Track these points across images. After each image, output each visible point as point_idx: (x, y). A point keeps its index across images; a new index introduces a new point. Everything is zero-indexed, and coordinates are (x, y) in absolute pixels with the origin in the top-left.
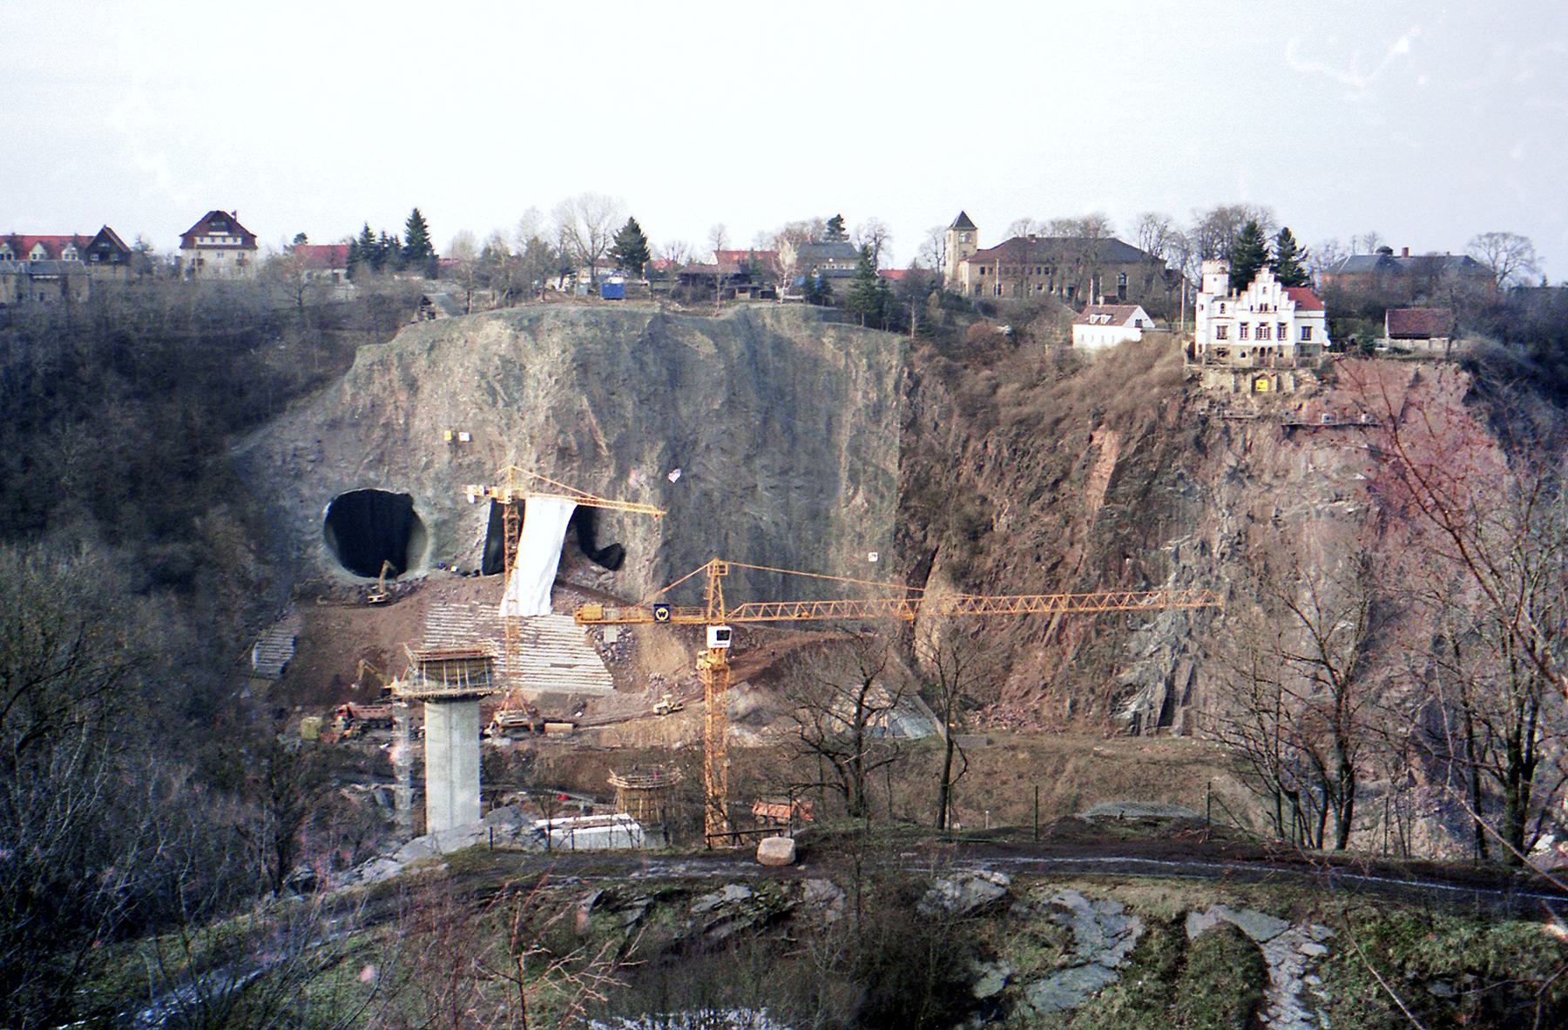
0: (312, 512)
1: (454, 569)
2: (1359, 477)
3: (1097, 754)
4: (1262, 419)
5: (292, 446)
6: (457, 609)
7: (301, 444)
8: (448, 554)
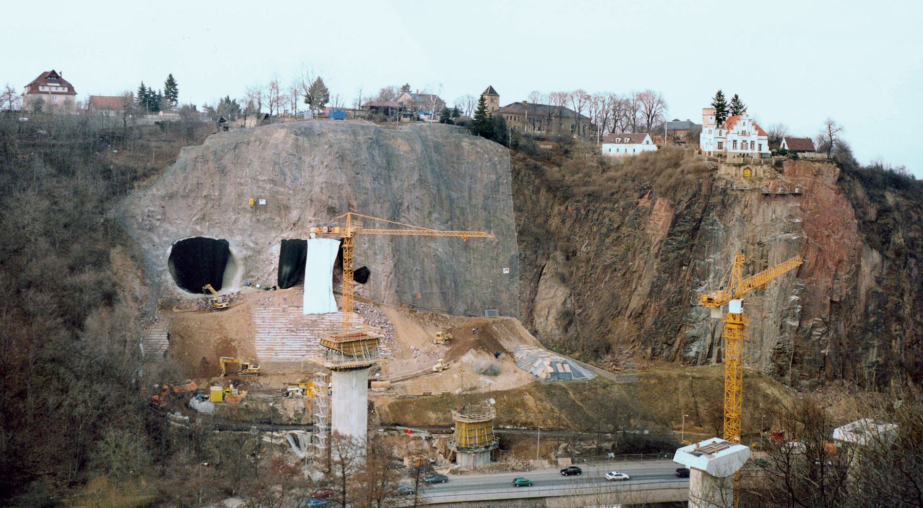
0: (161, 252)
1: (258, 286)
2: (797, 221)
3: (693, 378)
4: (753, 190)
5: (146, 210)
6: (274, 311)
7: (152, 209)
8: (252, 277)
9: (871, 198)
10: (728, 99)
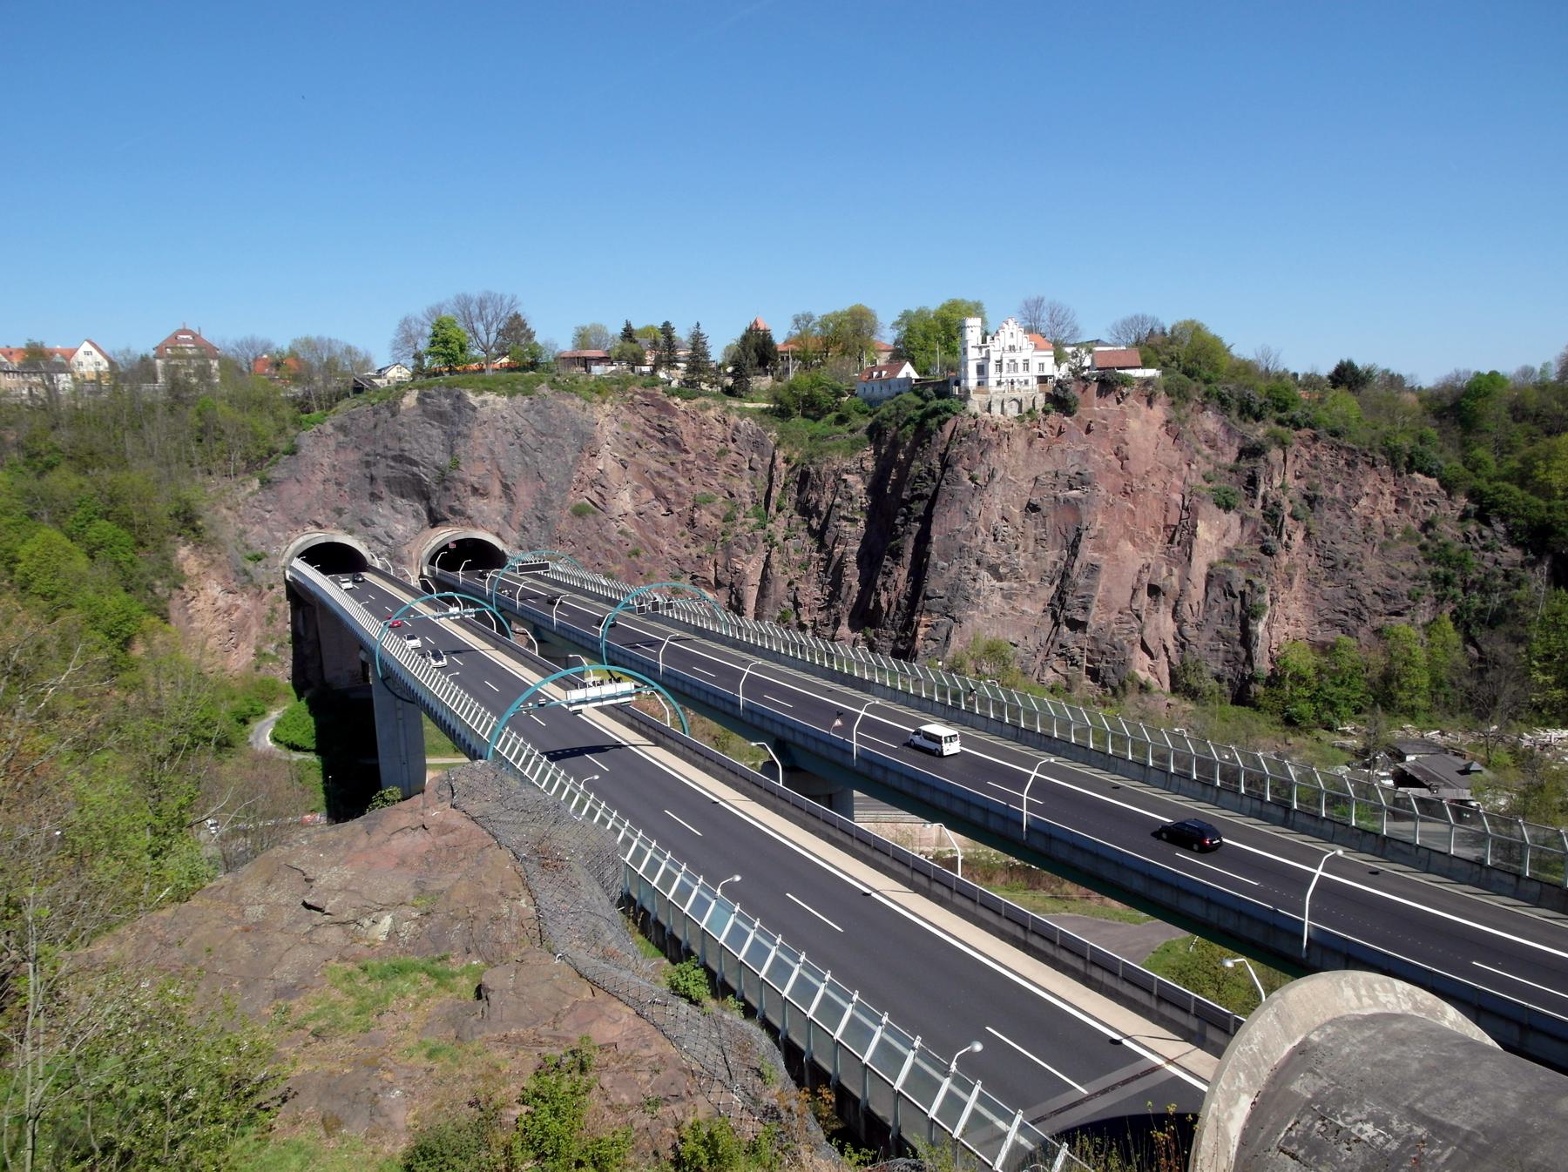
9: (1229, 431)
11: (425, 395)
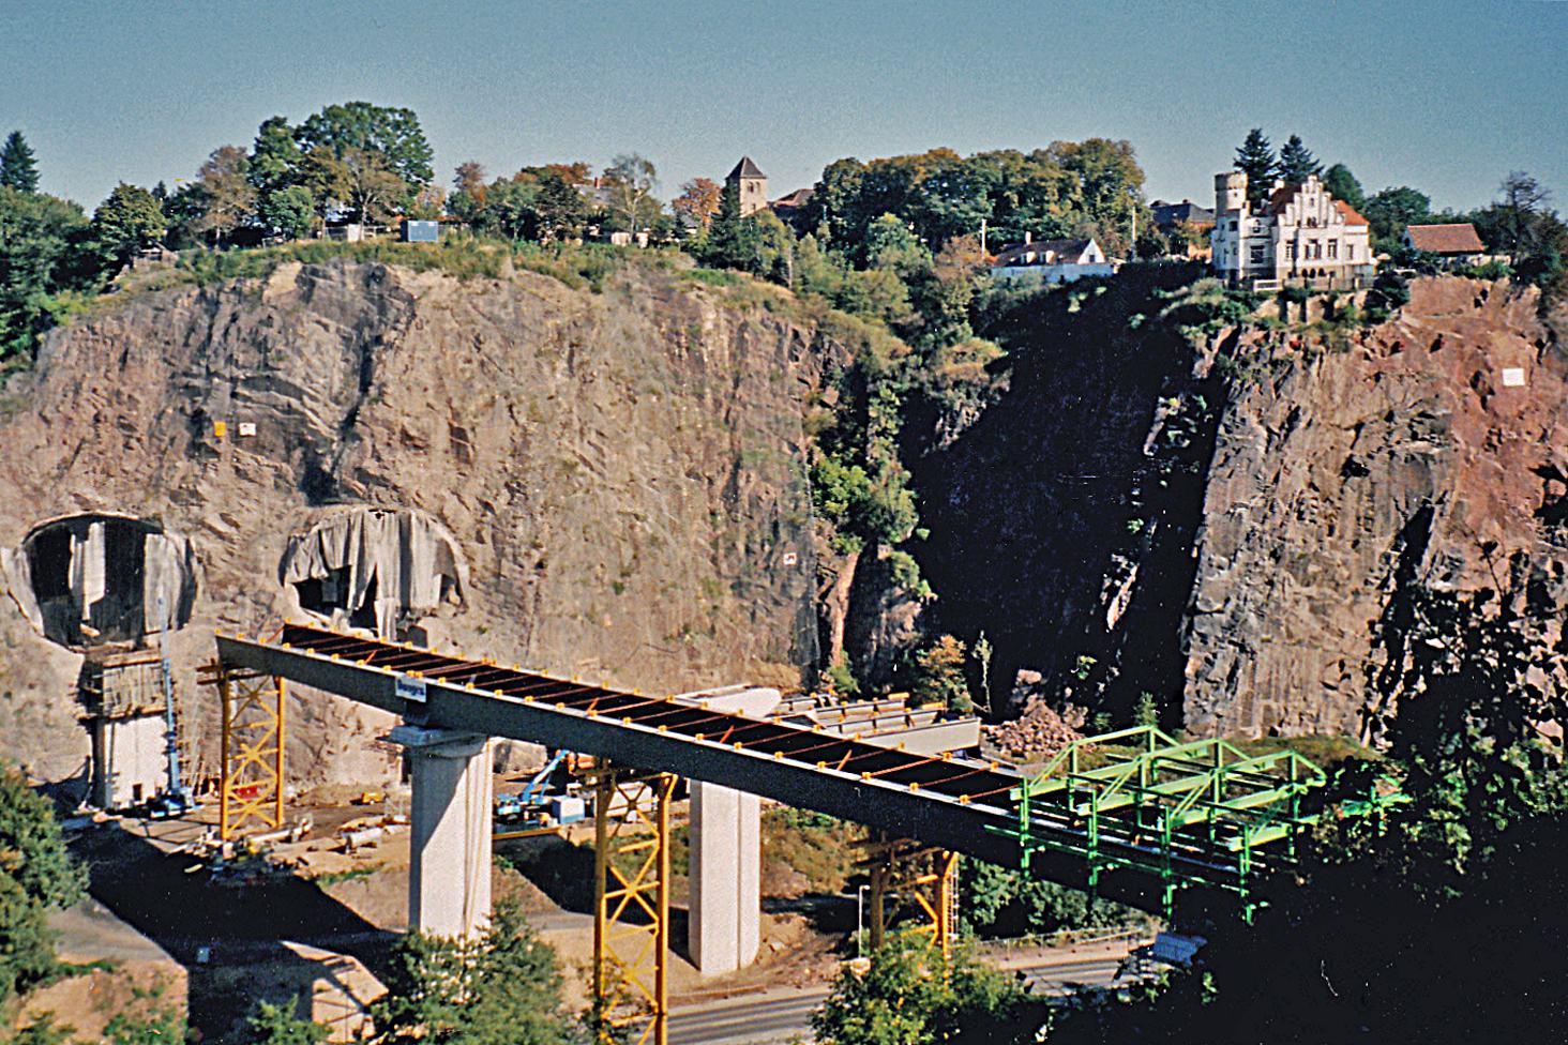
10: (1275, 150)
11: (314, 272)
